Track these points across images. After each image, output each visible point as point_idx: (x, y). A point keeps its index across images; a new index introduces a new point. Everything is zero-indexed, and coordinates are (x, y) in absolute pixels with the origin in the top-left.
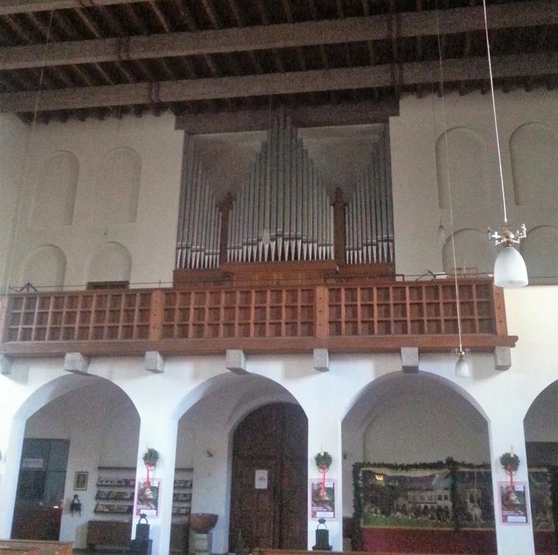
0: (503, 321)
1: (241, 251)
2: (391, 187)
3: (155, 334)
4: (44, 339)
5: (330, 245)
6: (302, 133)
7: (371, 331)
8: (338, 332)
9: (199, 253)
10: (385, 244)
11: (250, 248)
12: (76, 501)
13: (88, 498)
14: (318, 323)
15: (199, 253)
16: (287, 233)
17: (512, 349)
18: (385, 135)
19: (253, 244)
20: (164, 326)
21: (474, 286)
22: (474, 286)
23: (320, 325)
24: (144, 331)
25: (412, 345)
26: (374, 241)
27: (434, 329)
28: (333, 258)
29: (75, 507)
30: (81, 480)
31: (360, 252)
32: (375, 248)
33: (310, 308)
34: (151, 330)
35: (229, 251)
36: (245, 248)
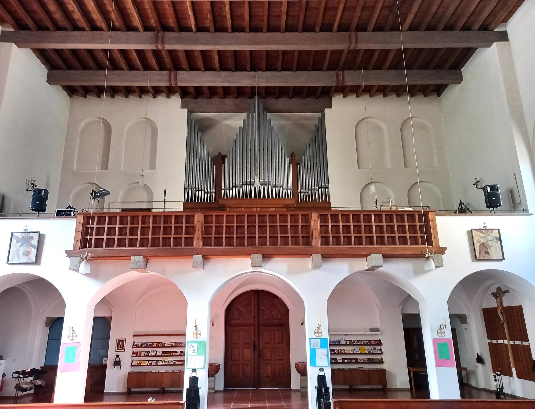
0: (436, 238)
3: (198, 243)
4: (114, 247)
7: (350, 243)
8: (327, 243)
9: (200, 192)
10: (323, 190)
11: (237, 189)
12: (118, 359)
13: (126, 357)
14: (314, 237)
17: (443, 256)
18: (322, 120)
19: (239, 187)
20: (204, 238)
21: (417, 216)
23: (315, 238)
24: (190, 242)
26: (317, 188)
29: (117, 363)
30: (121, 344)
33: (307, 228)
36: (234, 189)
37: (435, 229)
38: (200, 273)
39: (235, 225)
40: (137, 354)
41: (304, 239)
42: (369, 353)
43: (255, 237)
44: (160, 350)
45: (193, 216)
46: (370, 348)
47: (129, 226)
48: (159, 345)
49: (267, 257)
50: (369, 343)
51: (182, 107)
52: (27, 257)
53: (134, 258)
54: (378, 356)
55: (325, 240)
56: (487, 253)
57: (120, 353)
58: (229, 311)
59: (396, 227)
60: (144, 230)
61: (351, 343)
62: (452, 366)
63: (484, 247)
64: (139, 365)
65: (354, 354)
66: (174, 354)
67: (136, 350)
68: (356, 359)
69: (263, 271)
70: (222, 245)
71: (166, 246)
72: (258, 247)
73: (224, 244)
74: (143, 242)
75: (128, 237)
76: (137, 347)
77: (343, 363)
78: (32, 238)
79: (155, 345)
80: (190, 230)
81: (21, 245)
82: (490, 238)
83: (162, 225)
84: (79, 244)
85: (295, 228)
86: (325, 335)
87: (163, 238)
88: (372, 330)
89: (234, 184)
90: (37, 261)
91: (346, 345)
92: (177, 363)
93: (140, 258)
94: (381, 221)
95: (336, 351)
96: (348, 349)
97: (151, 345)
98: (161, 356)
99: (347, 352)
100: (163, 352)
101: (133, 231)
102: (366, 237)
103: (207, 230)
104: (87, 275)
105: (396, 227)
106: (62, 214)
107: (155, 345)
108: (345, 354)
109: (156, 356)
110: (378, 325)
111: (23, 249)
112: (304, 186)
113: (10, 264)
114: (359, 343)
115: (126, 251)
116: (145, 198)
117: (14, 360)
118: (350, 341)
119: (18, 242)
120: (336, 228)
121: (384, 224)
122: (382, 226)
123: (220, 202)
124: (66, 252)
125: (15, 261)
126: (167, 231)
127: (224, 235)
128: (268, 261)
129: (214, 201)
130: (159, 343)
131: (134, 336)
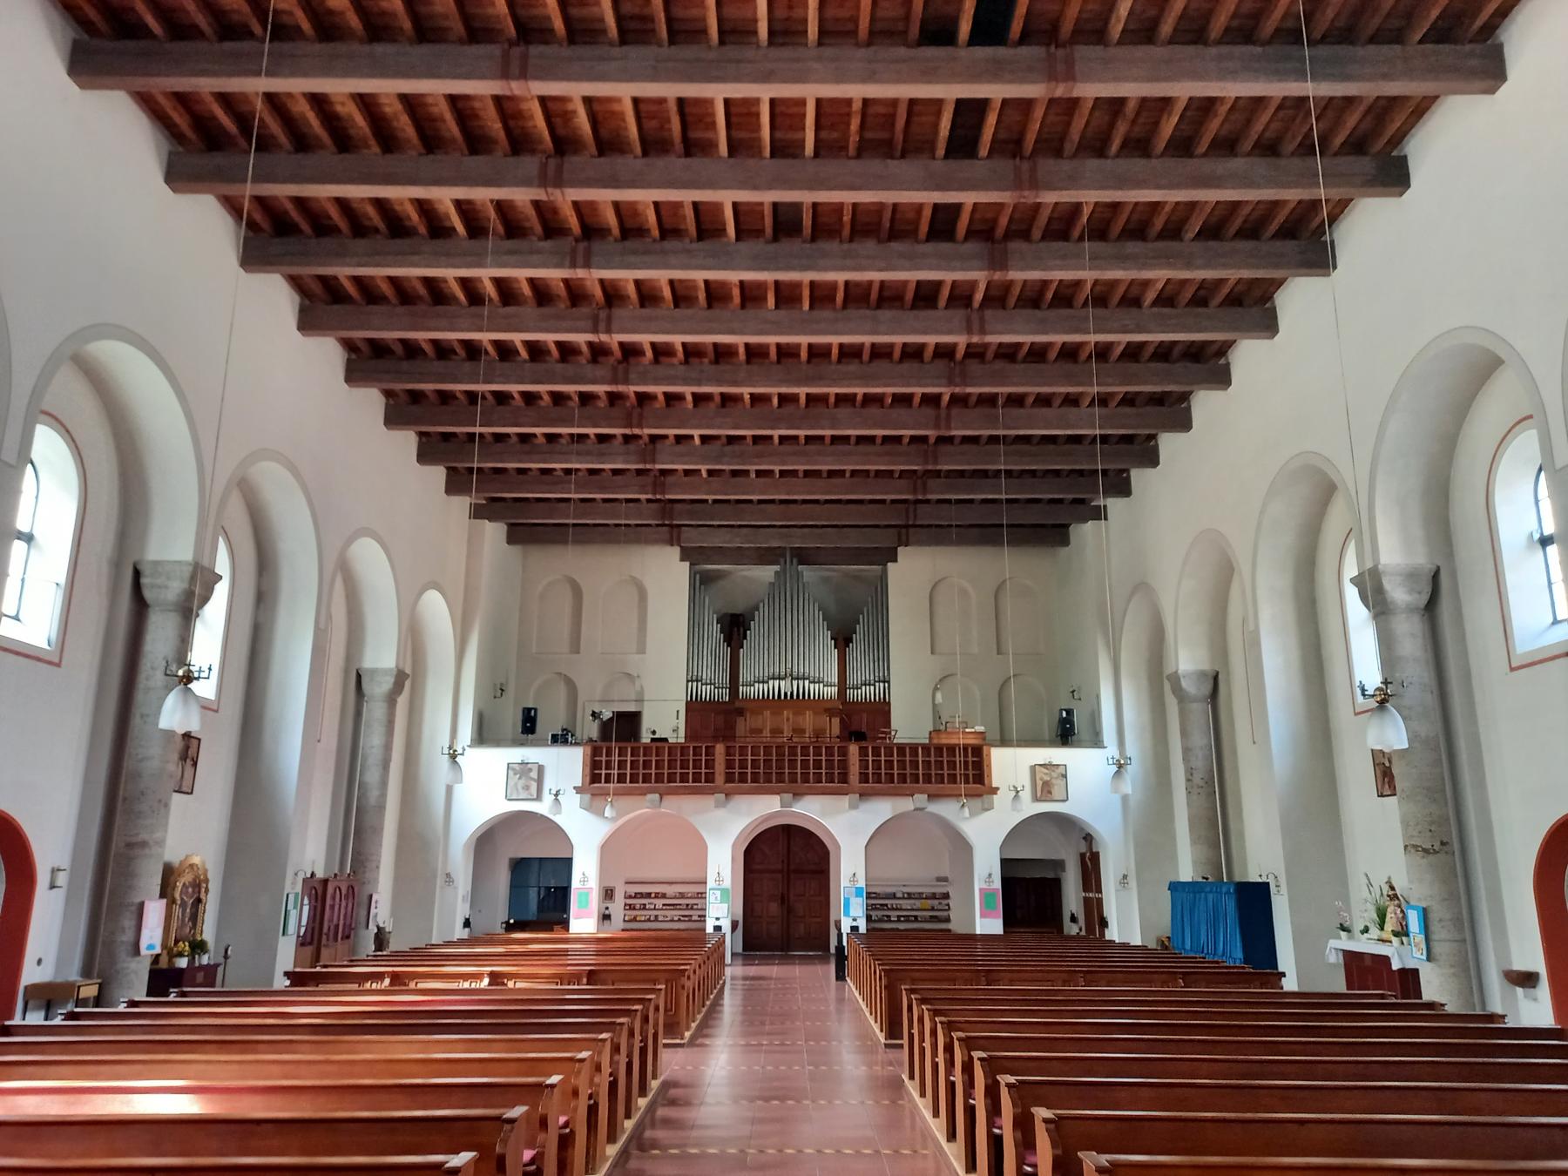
1: (752, 688)
3: (720, 778)
5: (835, 686)
10: (882, 685)
12: (607, 912)
15: (708, 687)
16: (795, 674)
19: (763, 682)
24: (710, 778)
25: (922, 793)
27: (939, 779)
31: (859, 691)
32: (872, 688)
33: (844, 764)
34: (717, 776)
35: (741, 688)
36: (756, 685)
38: (721, 813)
39: (762, 758)
40: (631, 907)
41: (841, 775)
42: (933, 909)
43: (784, 773)
44: (659, 903)
45: (714, 747)
46: (936, 902)
47: (641, 759)
48: (657, 896)
49: (797, 795)
50: (933, 896)
51: (682, 560)
52: (527, 792)
53: (650, 796)
54: (945, 913)
57: (608, 905)
58: (748, 853)
59: (945, 762)
60: (659, 765)
61: (910, 896)
62: (996, 917)
64: (634, 920)
65: (912, 910)
66: (678, 907)
68: (916, 917)
69: (793, 809)
70: (747, 782)
71: (683, 782)
73: (749, 781)
74: (659, 779)
76: (630, 897)
77: (899, 921)
78: (530, 770)
79: (653, 895)
81: (520, 778)
83: (679, 758)
84: (588, 779)
85: (830, 762)
86: (862, 883)
87: (681, 773)
88: (939, 879)
89: (756, 679)
90: (539, 798)
91: (904, 898)
92: (682, 918)
94: (929, 756)
95: (889, 906)
96: (906, 904)
97: (648, 895)
98: (662, 909)
99: (904, 907)
100: (664, 905)
101: (647, 765)
102: (911, 774)
103: (729, 764)
105: (945, 762)
106: (561, 739)
107: (653, 895)
108: (901, 909)
109: (655, 909)
110: (945, 871)
111: (522, 783)
112: (854, 678)
113: (509, 800)
114: (920, 896)
117: (480, 911)
118: (908, 894)
119: (515, 774)
120: (877, 764)
121: (932, 759)
122: (930, 761)
123: (737, 704)
124: (575, 788)
126: (684, 765)
127: (749, 770)
128: (799, 800)
129: (727, 700)
130: (658, 893)
131: (626, 883)
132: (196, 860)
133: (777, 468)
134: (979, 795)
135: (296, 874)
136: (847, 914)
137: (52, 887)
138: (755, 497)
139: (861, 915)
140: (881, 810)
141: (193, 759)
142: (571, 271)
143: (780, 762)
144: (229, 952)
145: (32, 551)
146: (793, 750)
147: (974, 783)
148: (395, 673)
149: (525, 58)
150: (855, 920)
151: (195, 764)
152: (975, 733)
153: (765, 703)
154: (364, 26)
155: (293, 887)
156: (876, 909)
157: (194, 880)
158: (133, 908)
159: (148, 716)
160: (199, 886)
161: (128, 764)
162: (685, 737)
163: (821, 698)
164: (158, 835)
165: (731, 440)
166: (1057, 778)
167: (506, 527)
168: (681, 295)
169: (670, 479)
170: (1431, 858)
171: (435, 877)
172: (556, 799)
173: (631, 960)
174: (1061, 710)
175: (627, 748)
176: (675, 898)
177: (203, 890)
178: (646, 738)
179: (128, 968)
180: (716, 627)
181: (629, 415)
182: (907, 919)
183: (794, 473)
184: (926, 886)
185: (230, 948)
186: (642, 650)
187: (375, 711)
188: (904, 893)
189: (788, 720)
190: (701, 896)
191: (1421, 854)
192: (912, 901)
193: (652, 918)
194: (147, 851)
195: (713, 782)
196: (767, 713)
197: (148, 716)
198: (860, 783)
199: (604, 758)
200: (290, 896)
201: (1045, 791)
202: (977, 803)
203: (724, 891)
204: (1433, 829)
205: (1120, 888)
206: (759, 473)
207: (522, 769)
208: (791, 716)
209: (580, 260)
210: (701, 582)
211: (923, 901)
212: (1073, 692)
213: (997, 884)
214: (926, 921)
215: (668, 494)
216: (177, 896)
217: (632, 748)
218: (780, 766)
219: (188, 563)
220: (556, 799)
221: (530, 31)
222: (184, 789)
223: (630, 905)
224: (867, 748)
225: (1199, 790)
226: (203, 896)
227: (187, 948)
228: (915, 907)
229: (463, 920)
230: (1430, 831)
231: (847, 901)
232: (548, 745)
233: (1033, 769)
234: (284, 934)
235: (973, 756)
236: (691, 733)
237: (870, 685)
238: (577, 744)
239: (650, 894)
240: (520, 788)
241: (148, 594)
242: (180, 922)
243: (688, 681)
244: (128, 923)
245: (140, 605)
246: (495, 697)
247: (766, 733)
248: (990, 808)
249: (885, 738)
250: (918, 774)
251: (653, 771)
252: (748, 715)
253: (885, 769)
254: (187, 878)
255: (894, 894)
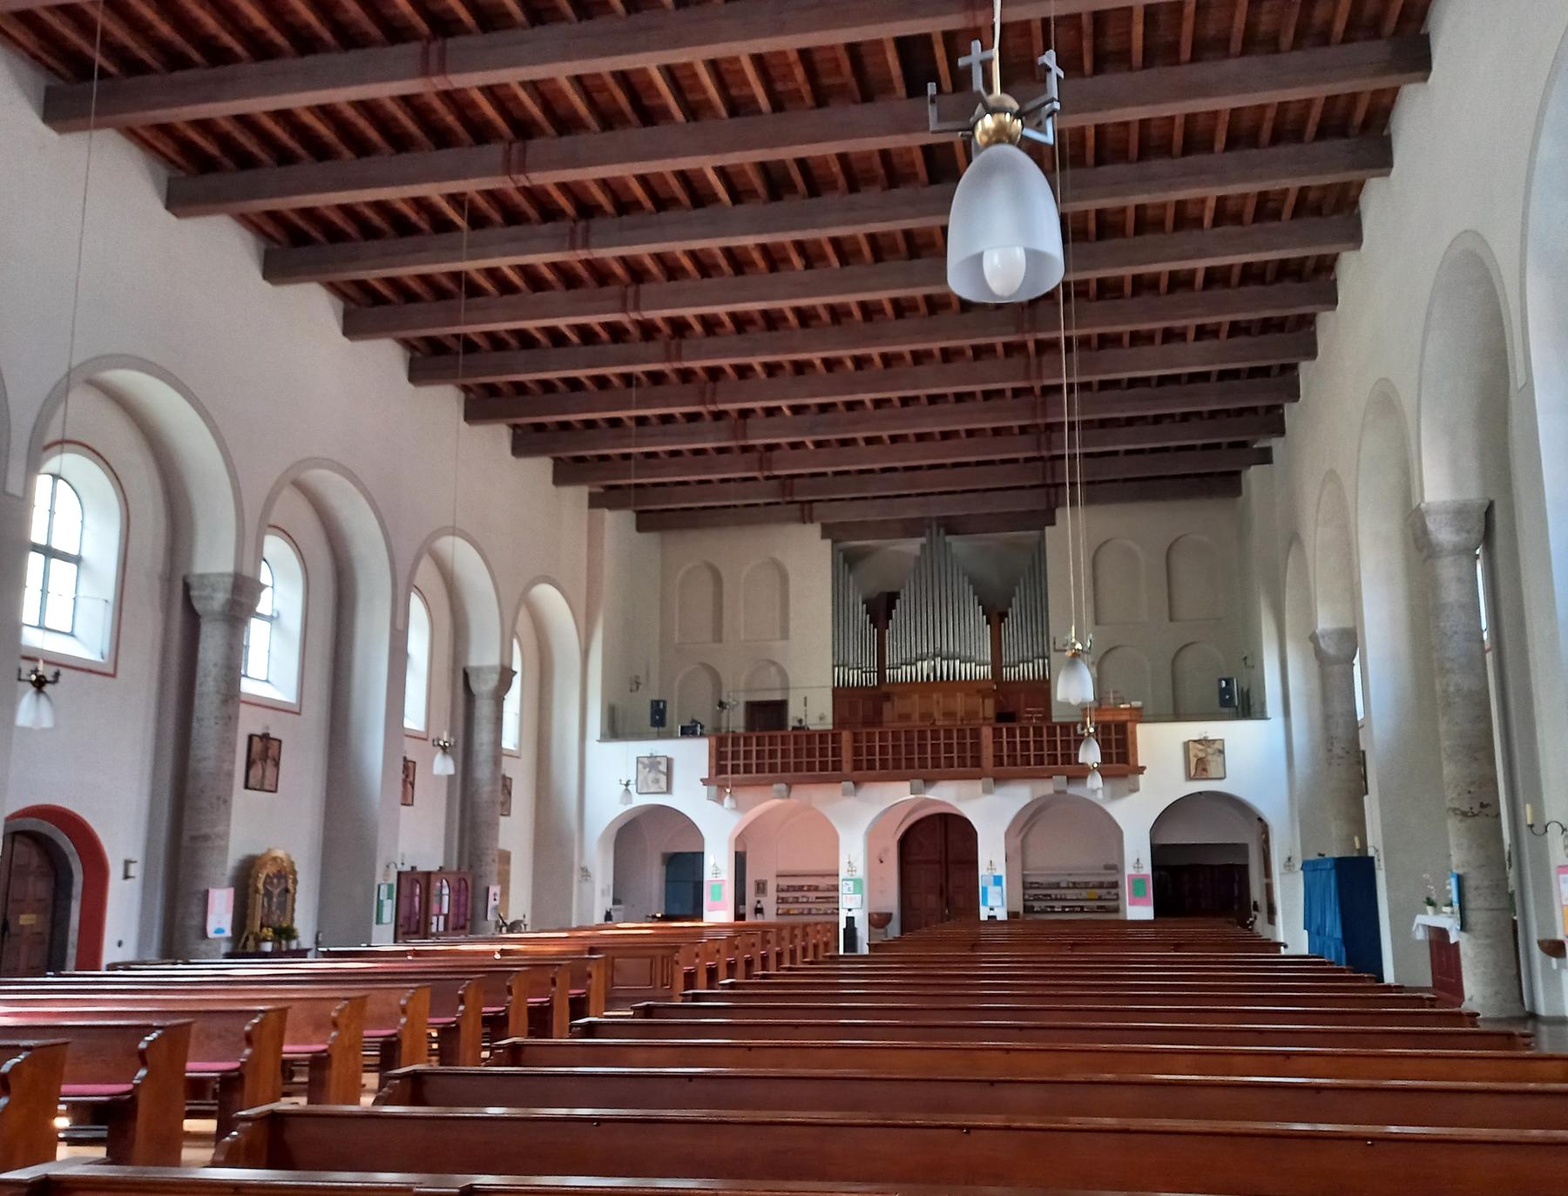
1: (899, 671)
2: (1046, 580)
3: (847, 767)
6: (948, 538)
8: (1002, 764)
12: (759, 906)
16: (944, 654)
19: (911, 664)
21: (1113, 727)
22: (1113, 727)
24: (837, 766)
28: (990, 677)
33: (977, 746)
35: (887, 671)
36: (904, 667)
37: (1135, 744)
38: (850, 802)
42: (1100, 899)
44: (812, 895)
45: (840, 734)
46: (1103, 892)
47: (767, 748)
49: (929, 781)
50: (1101, 886)
51: (824, 537)
53: (776, 786)
55: (998, 761)
56: (1205, 770)
57: (763, 899)
58: (905, 843)
61: (1075, 886)
63: (1201, 762)
64: (787, 913)
67: (783, 895)
68: (1082, 907)
72: (917, 771)
74: (785, 768)
75: (767, 761)
76: (783, 891)
77: (1063, 912)
78: (659, 763)
80: (836, 752)
81: (649, 772)
82: (1209, 750)
83: (804, 746)
84: (714, 771)
85: (961, 745)
87: (808, 762)
88: (1108, 867)
90: (669, 790)
91: (1068, 888)
93: (783, 787)
96: (1070, 894)
97: (801, 888)
99: (1068, 897)
100: (817, 898)
101: (772, 754)
102: (1049, 755)
103: (856, 751)
104: (733, 809)
106: (688, 731)
108: (1066, 900)
114: (1086, 886)
115: (766, 778)
116: (777, 683)
118: (1074, 883)
119: (645, 768)
120: (1012, 745)
123: (884, 689)
124: (702, 780)
125: (644, 791)
126: (810, 754)
132: (279, 853)
133: (885, 434)
134: (1125, 776)
135: (388, 866)
136: (985, 904)
137: (126, 877)
138: (876, 466)
139: (1000, 904)
140: (1017, 796)
141: (274, 760)
142: (572, 253)
143: (909, 746)
144: (320, 939)
145: (82, 572)
146: (922, 733)
147: (1118, 762)
148: (499, 670)
149: (442, 54)
150: (992, 909)
151: (277, 764)
152: (1131, 708)
153: (912, 686)
154: (290, 41)
155: (385, 880)
156: (1039, 900)
157: (279, 871)
158: (199, 896)
159: (202, 720)
160: (285, 878)
161: (192, 765)
162: (834, 724)
163: (963, 678)
164: (220, 829)
165: (823, 408)
166: (1213, 754)
167: (634, 515)
168: (704, 265)
169: (776, 454)
170: (1470, 821)
171: (571, 871)
172: (627, 790)
173: (661, 940)
174: (1220, 680)
175: (764, 737)
176: (828, 890)
177: (290, 881)
178: (792, 723)
179: (198, 949)
180: (862, 608)
181: (702, 393)
182: (1073, 910)
183: (903, 438)
184: (1093, 874)
185: (321, 935)
186: (785, 634)
187: (484, 709)
188: (1068, 883)
189: (938, 703)
190: (836, 888)
191: (1460, 817)
192: (1077, 891)
193: (806, 912)
194: (209, 844)
195: (840, 770)
196: (916, 697)
197: (202, 720)
198: (995, 766)
199: (730, 749)
200: (382, 887)
201: (1200, 768)
202: (1122, 784)
203: (857, 882)
204: (1472, 790)
205: (1284, 871)
206: (869, 441)
207: (652, 763)
208: (941, 700)
209: (579, 241)
210: (847, 562)
211: (1089, 890)
212: (1245, 658)
213: (1147, 869)
214: (1092, 912)
215: (776, 469)
216: (260, 886)
217: (758, 738)
218: (910, 751)
219: (229, 575)
220: (627, 790)
221: (444, 26)
222: (267, 787)
223: (783, 898)
224: (1014, 729)
225: (1340, 761)
226: (290, 886)
227: (271, 934)
228: (1080, 897)
229: (604, 913)
230: (1469, 792)
231: (985, 889)
232: (677, 738)
233: (1186, 745)
234: (377, 923)
235: (1116, 734)
236: (839, 721)
237: (1028, 662)
238: (702, 735)
239: (803, 886)
240: (650, 783)
241: (198, 606)
242: (266, 910)
243: (834, 667)
244: (195, 909)
245: (193, 620)
246: (631, 691)
247: (916, 716)
248: (1135, 790)
249: (1032, 718)
250: (1056, 755)
251: (779, 761)
252: (896, 699)
253: (1035, 750)
254: (270, 869)
255: (1058, 883)
